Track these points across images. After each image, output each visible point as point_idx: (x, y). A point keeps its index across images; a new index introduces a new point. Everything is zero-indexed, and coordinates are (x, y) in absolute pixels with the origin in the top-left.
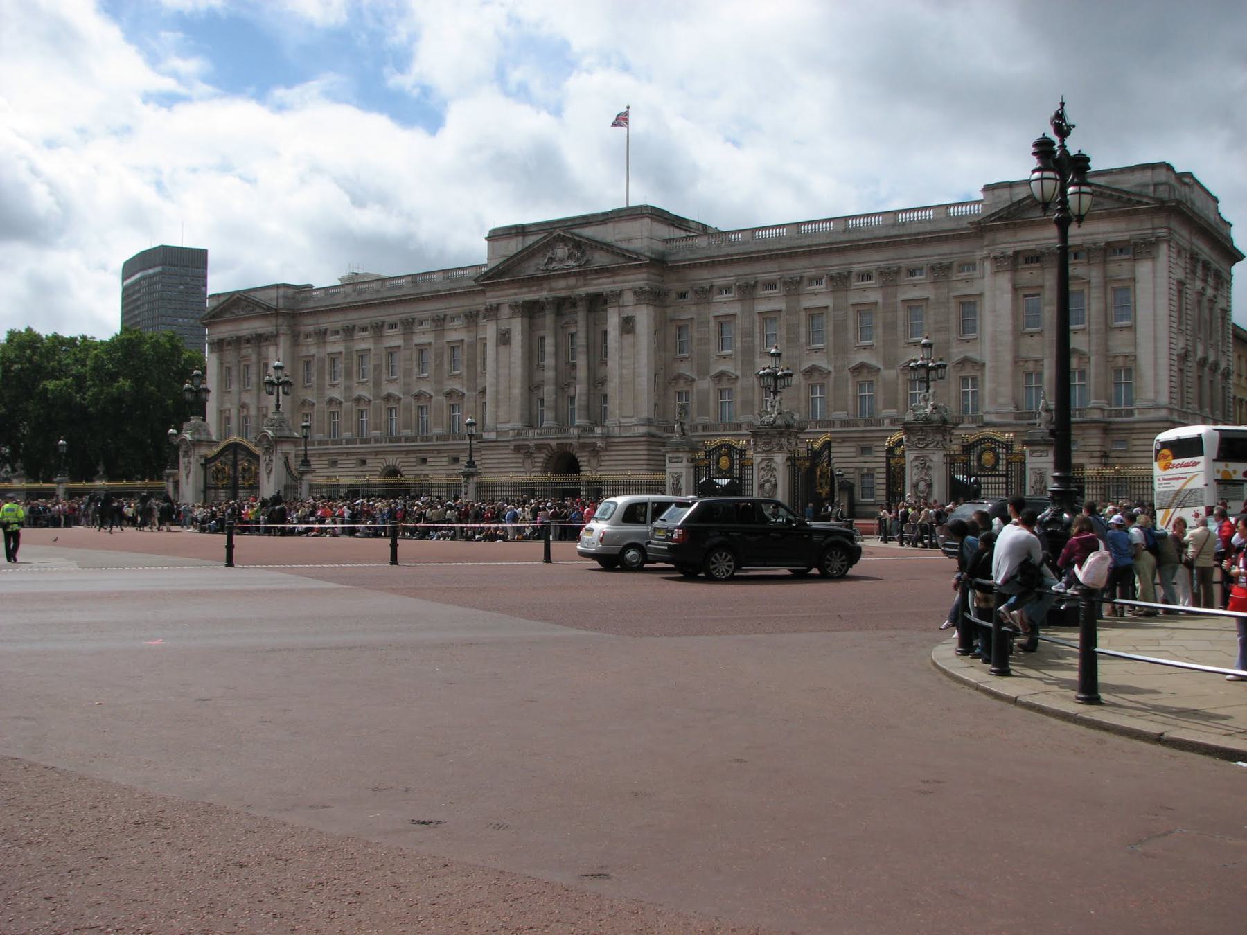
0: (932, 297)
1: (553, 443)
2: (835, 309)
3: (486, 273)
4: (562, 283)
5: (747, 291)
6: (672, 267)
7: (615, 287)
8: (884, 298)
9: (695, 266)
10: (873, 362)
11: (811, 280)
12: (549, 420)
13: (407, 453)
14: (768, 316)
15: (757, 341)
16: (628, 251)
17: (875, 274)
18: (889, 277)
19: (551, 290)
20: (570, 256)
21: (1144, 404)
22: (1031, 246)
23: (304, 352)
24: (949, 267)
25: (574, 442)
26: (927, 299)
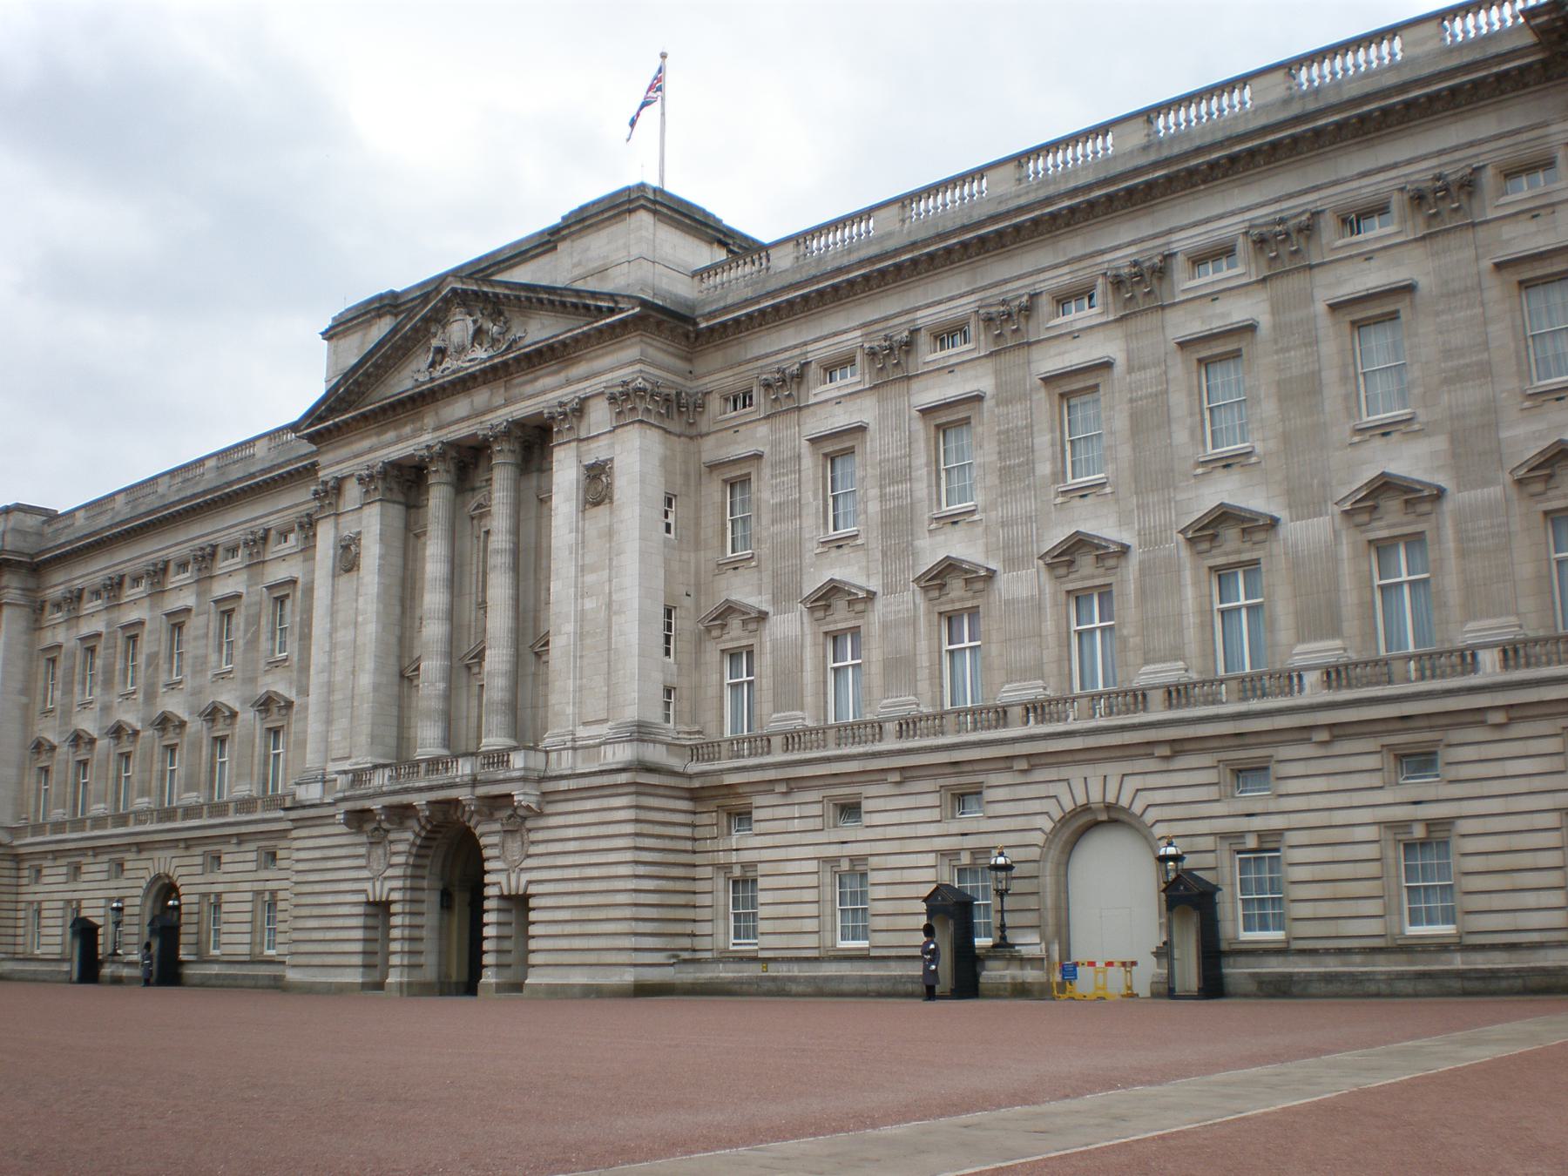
0: (1424, 283)
1: (419, 800)
2: (1130, 370)
4: (460, 407)
5: (892, 359)
6: (711, 329)
7: (569, 394)
8: (1275, 311)
10: (1257, 501)
11: (1063, 300)
12: (428, 739)
13: (189, 844)
15: (921, 489)
23: (49, 638)
24: (1469, 185)
25: (463, 794)
26: (1409, 289)
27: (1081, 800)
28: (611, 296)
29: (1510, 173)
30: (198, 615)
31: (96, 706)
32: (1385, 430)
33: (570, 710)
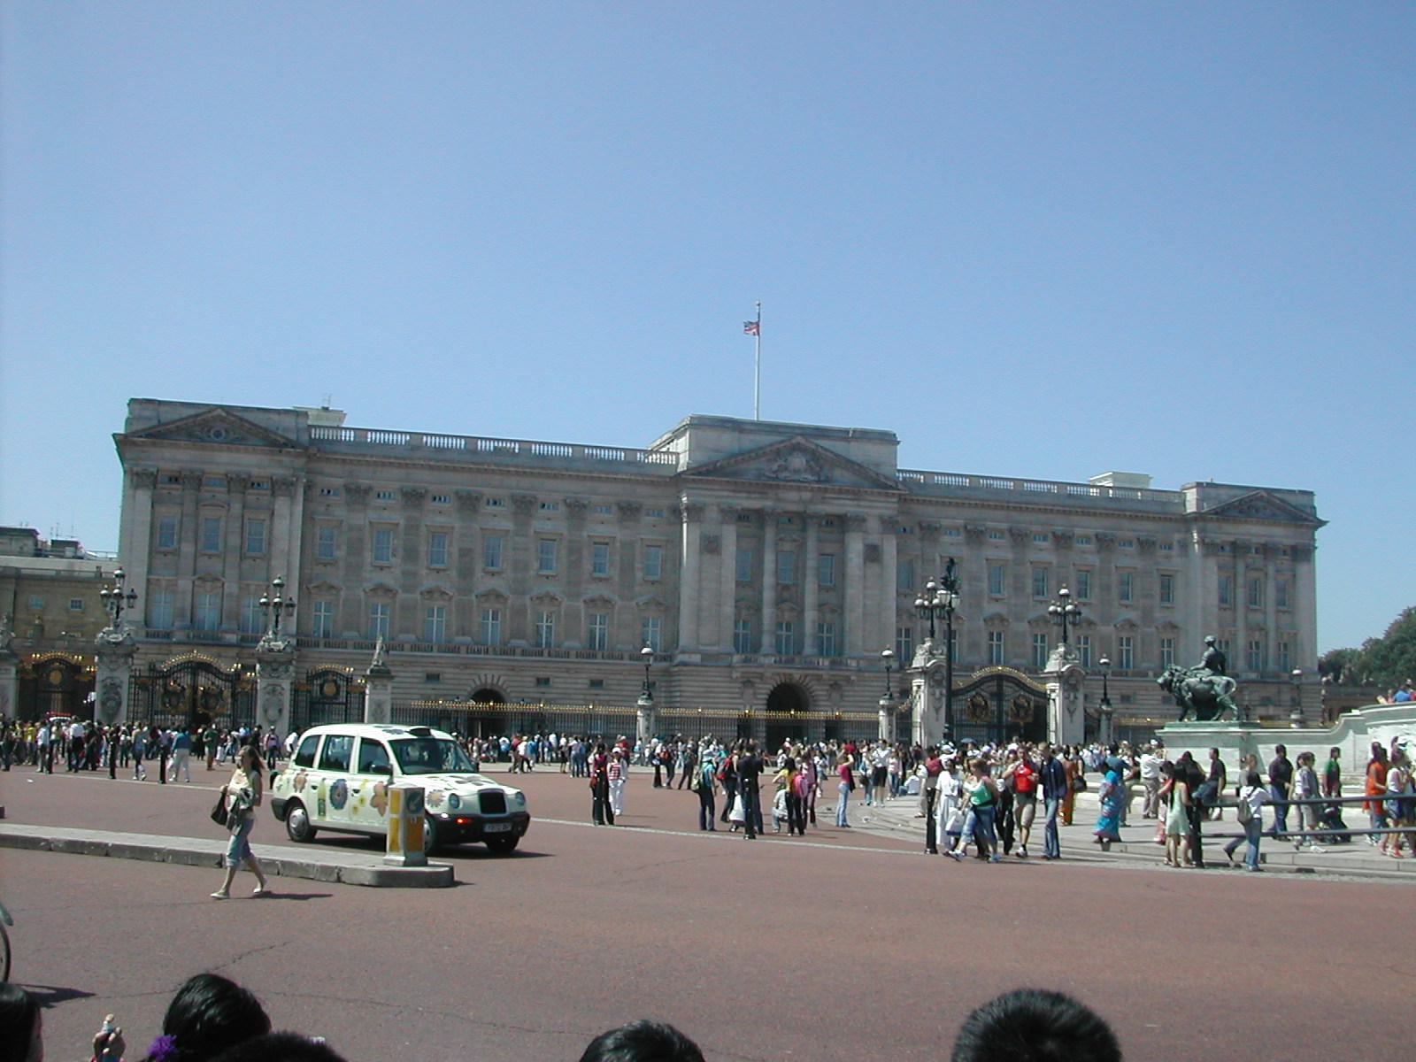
4: (793, 495)
5: (975, 536)
16: (886, 478)
17: (1094, 539)
18: (1105, 543)
20: (810, 469)
24: (1154, 543)
25: (825, 675)
30: (517, 535)
33: (860, 644)
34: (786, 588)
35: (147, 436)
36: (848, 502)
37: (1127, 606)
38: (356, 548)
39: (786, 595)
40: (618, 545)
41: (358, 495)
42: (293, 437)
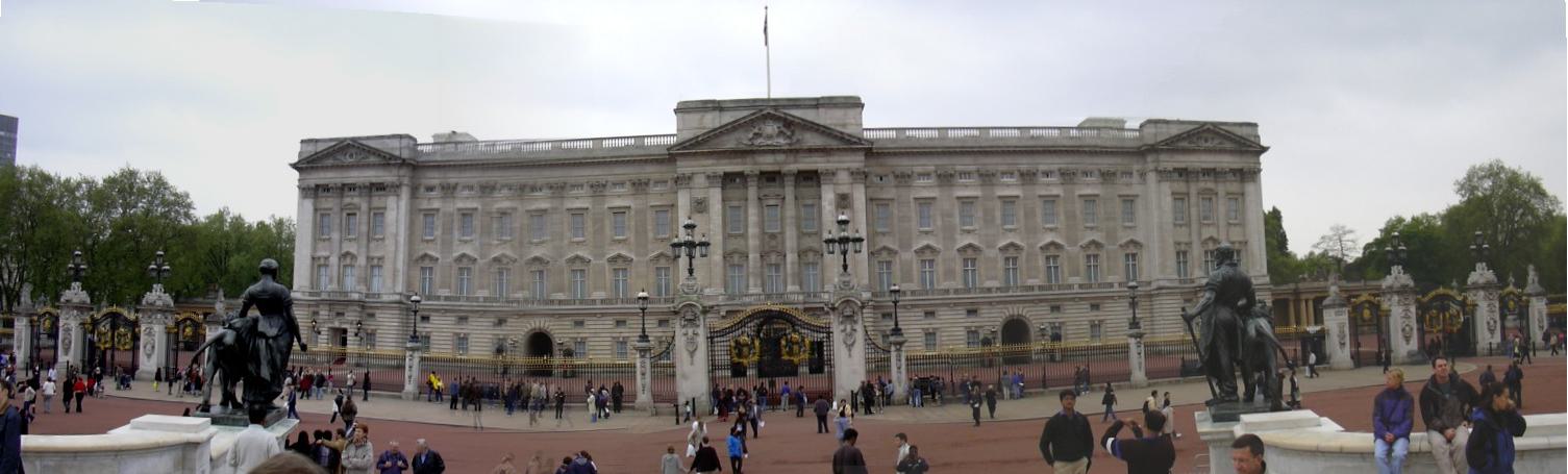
3: (675, 146)
4: (769, 159)
5: (946, 179)
6: (877, 153)
7: (830, 166)
8: (1065, 191)
9: (895, 154)
11: (1004, 173)
14: (965, 200)
15: (957, 220)
16: (849, 135)
17: (1057, 173)
18: (1067, 176)
19: (755, 164)
20: (781, 133)
21: (1256, 274)
22: (1183, 165)
24: (1114, 174)
26: (1097, 196)
27: (1011, 313)
28: (860, 140)
29: (1123, 173)
31: (477, 243)
32: (1092, 228)
34: (773, 236)
35: (308, 162)
36: (819, 159)
37: (1092, 228)
38: (448, 230)
39: (773, 243)
40: (633, 213)
41: (449, 190)
42: (397, 153)
